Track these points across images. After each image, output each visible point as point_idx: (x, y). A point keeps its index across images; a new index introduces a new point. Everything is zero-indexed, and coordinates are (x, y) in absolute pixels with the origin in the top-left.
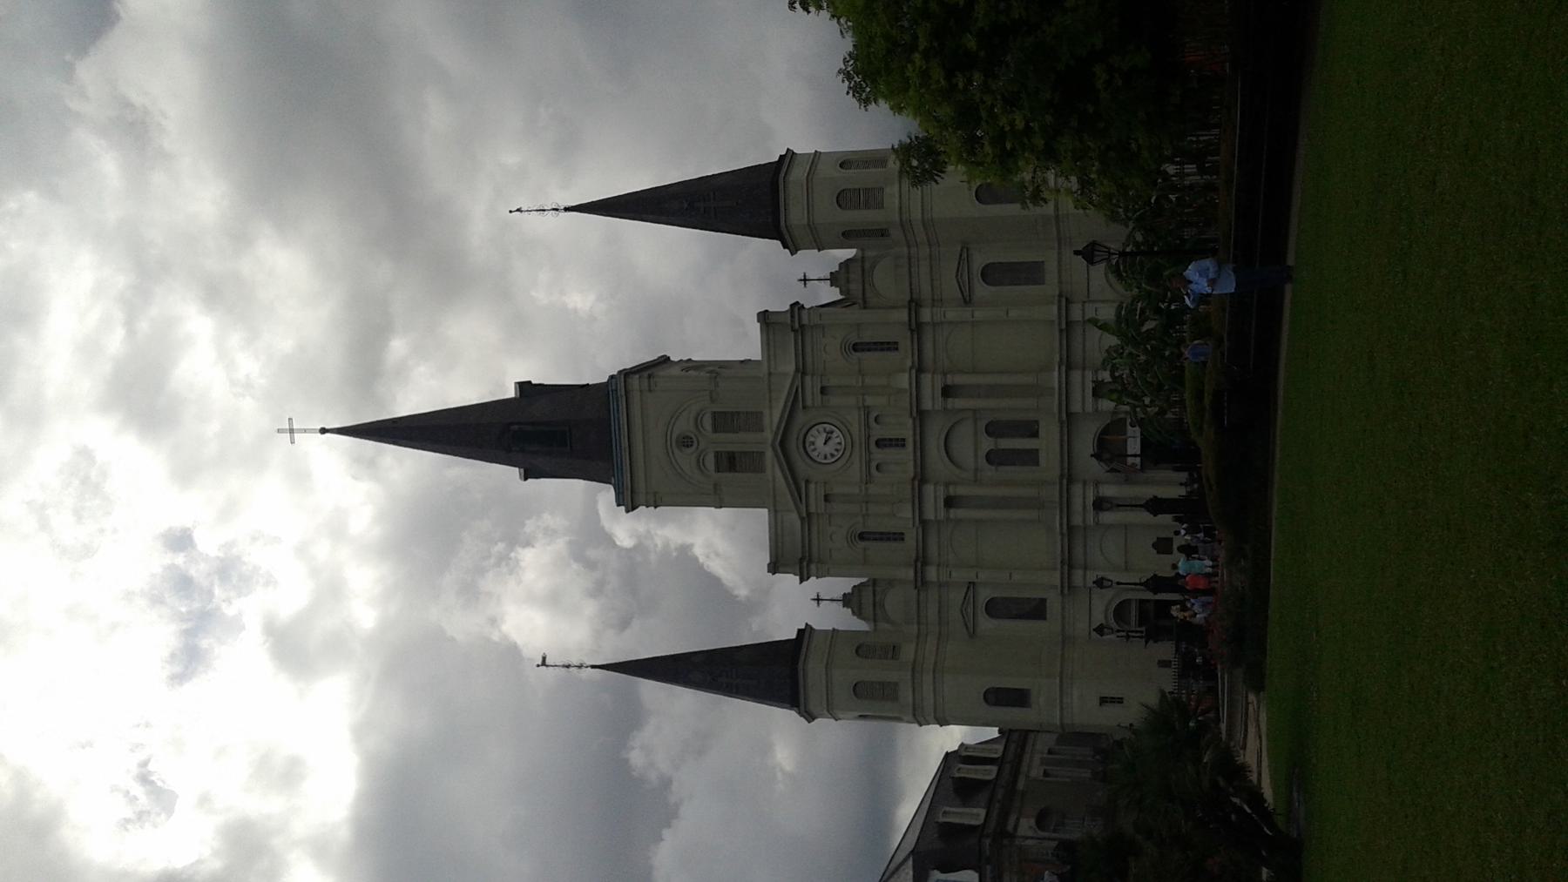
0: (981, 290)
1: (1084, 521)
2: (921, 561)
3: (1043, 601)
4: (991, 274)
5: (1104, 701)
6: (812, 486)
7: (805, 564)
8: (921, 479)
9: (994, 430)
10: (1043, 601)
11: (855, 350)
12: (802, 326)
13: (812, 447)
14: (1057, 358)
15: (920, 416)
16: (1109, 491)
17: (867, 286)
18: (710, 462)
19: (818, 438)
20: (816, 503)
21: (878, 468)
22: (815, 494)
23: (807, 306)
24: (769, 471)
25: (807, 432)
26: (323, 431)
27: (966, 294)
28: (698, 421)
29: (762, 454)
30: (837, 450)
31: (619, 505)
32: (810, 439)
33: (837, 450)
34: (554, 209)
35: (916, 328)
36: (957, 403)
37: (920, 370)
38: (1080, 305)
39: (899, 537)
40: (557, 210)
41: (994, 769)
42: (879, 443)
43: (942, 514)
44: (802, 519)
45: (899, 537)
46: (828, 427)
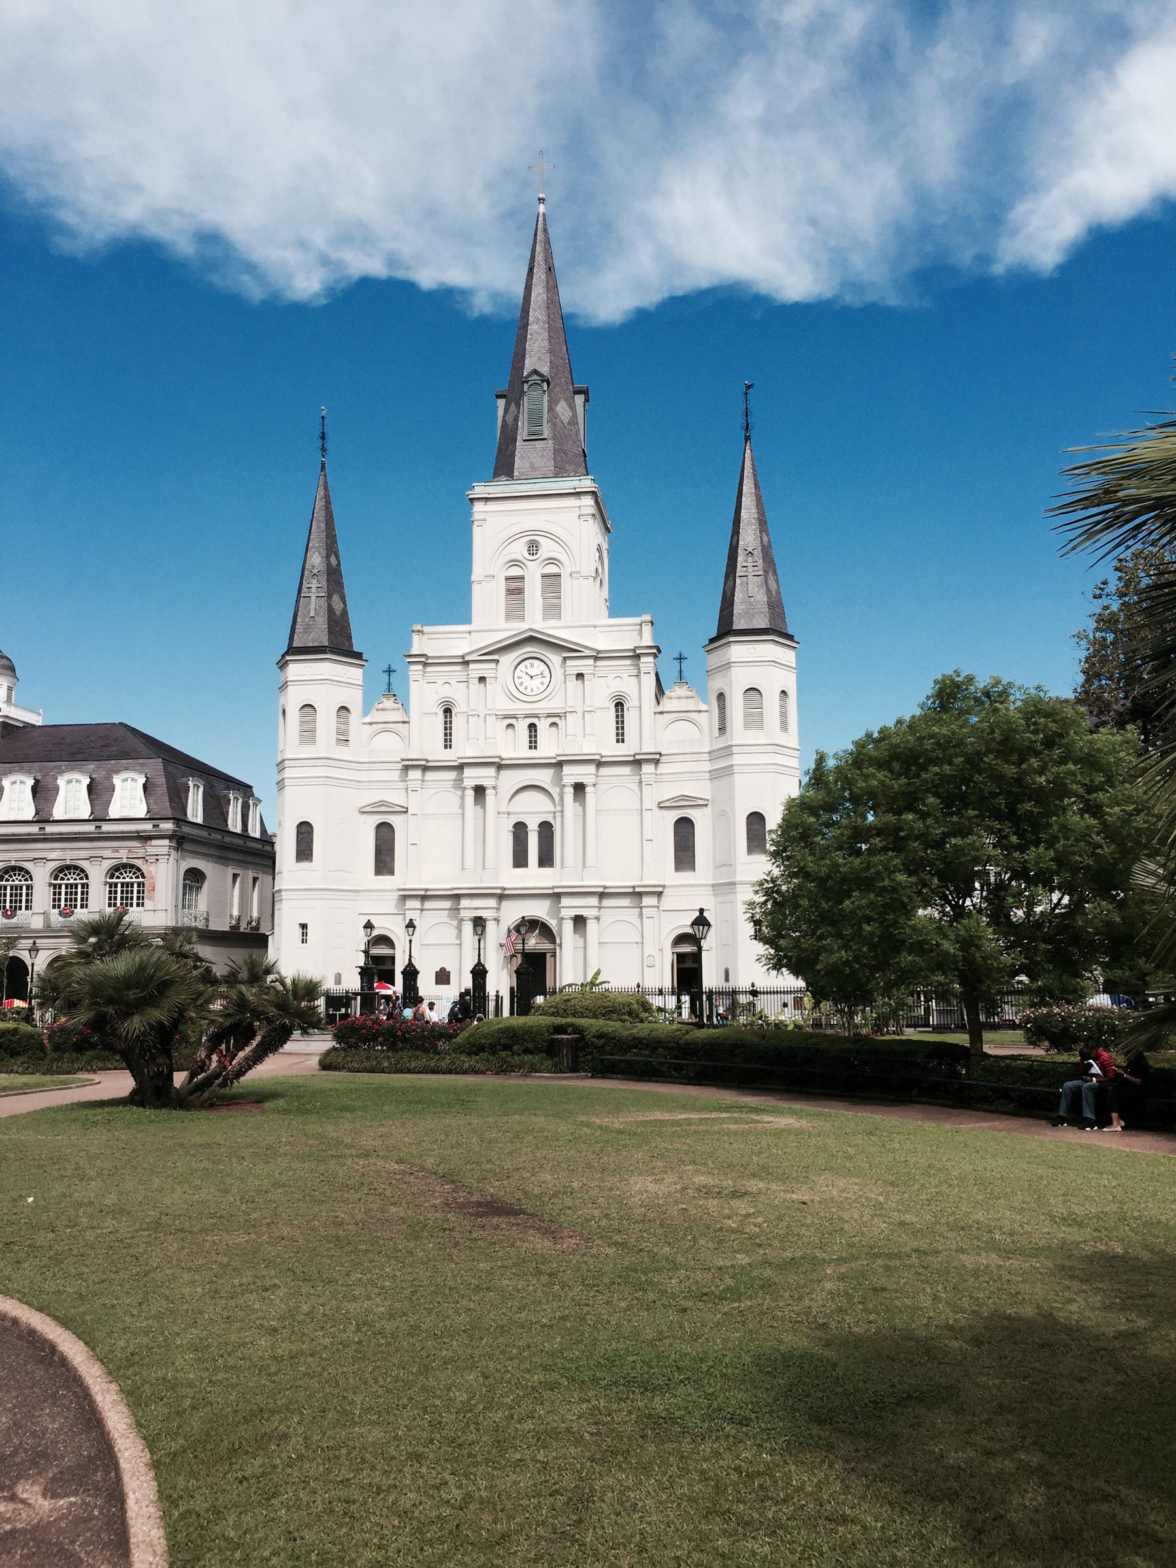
1: (465, 908)
3: (392, 872)
4: (684, 828)
5: (304, 926)
6: (493, 665)
7: (423, 659)
9: (546, 829)
10: (392, 872)
11: (617, 705)
12: (638, 657)
13: (529, 665)
14: (607, 884)
16: (491, 927)
17: (676, 715)
18: (515, 572)
19: (538, 667)
20: (476, 670)
25: (542, 660)
27: (668, 804)
28: (552, 561)
29: (522, 618)
30: (526, 688)
32: (536, 663)
33: (526, 688)
34: (747, 425)
35: (637, 763)
37: (599, 764)
38: (657, 904)
39: (448, 744)
40: (747, 428)
41: (239, 830)
42: (532, 727)
43: (469, 783)
44: (463, 657)
45: (448, 744)
46: (547, 680)
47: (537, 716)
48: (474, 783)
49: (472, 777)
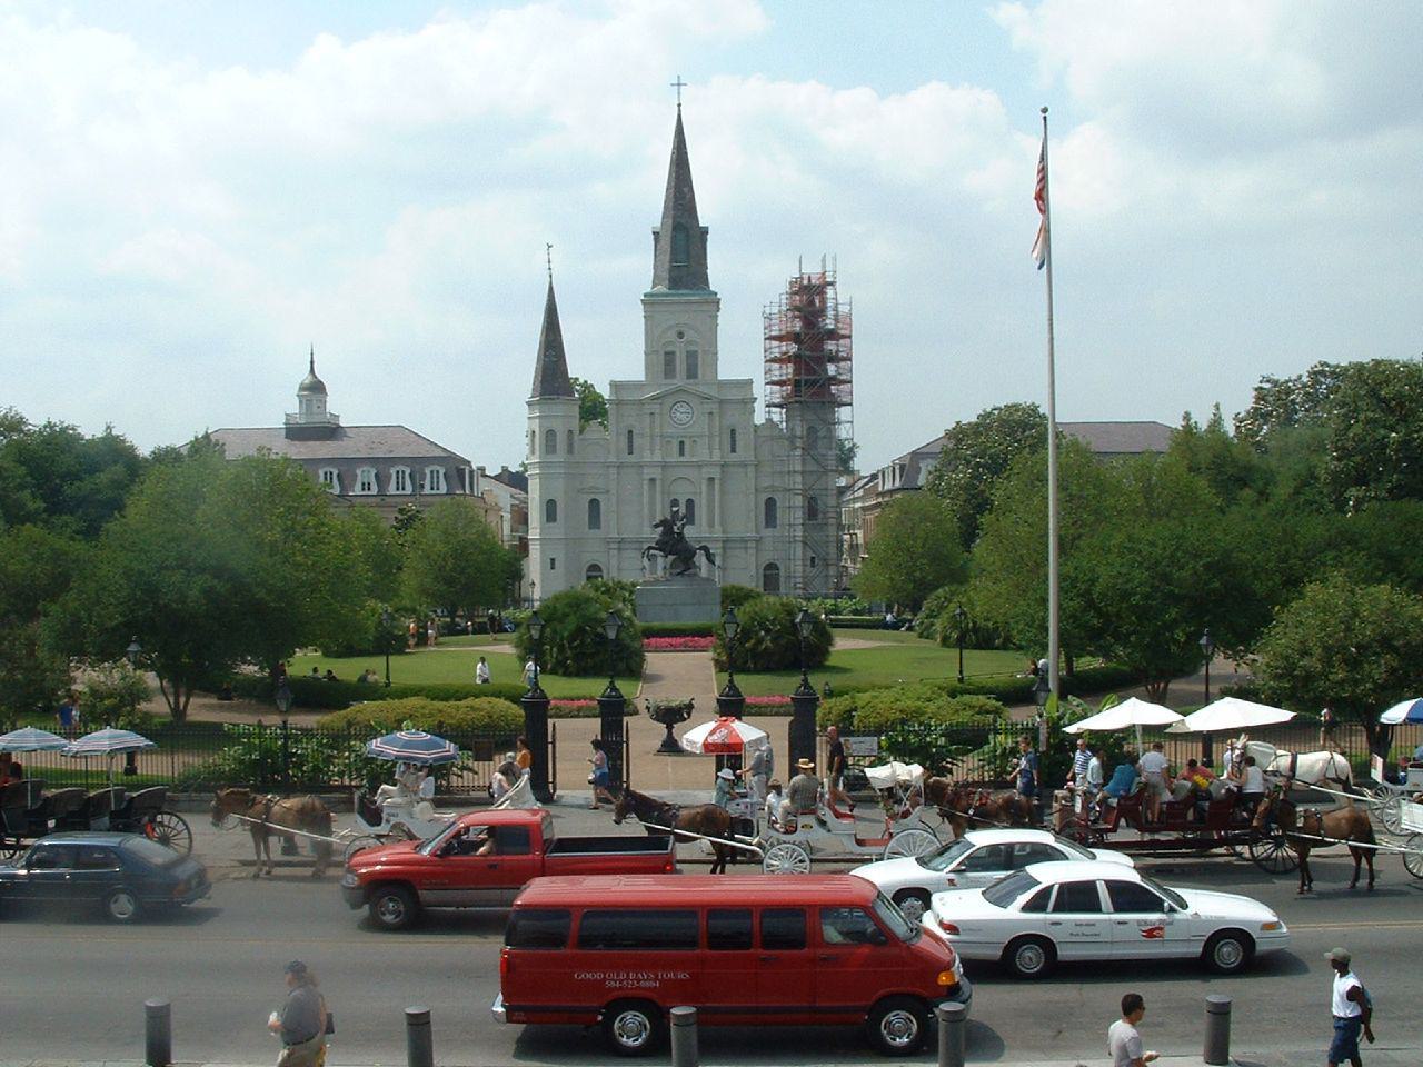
0: (764, 497)
2: (620, 466)
3: (599, 528)
5: (553, 560)
8: (665, 466)
15: (699, 465)
18: (670, 349)
21: (669, 442)
22: (656, 408)
23: (755, 405)
24: (668, 381)
26: (679, 105)
28: (690, 343)
31: (645, 295)
35: (744, 465)
36: (704, 483)
42: (682, 443)
47: (685, 437)
48: (649, 477)
49: (648, 473)
